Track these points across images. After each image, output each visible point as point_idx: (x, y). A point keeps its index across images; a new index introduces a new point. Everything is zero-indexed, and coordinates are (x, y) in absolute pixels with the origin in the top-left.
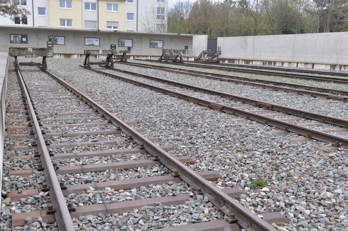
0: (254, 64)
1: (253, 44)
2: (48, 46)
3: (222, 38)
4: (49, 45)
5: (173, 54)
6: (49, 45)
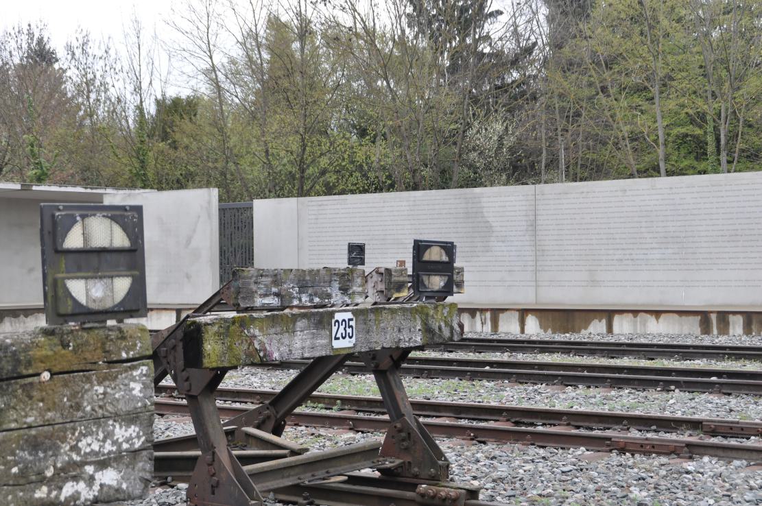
0: (624, 329)
1: (533, 226)
2: (55, 295)
3: (290, 204)
4: (78, 289)
5: (296, 302)
6: (78, 289)
